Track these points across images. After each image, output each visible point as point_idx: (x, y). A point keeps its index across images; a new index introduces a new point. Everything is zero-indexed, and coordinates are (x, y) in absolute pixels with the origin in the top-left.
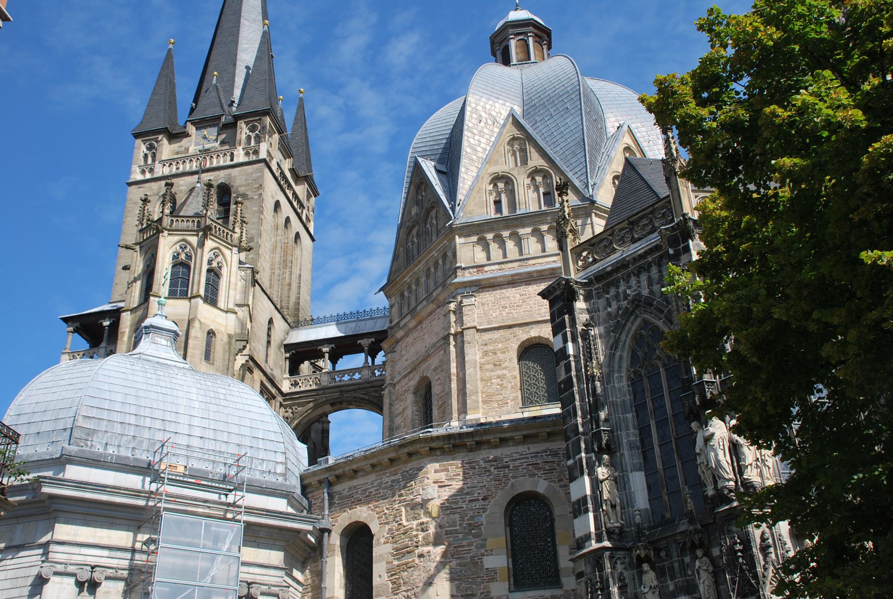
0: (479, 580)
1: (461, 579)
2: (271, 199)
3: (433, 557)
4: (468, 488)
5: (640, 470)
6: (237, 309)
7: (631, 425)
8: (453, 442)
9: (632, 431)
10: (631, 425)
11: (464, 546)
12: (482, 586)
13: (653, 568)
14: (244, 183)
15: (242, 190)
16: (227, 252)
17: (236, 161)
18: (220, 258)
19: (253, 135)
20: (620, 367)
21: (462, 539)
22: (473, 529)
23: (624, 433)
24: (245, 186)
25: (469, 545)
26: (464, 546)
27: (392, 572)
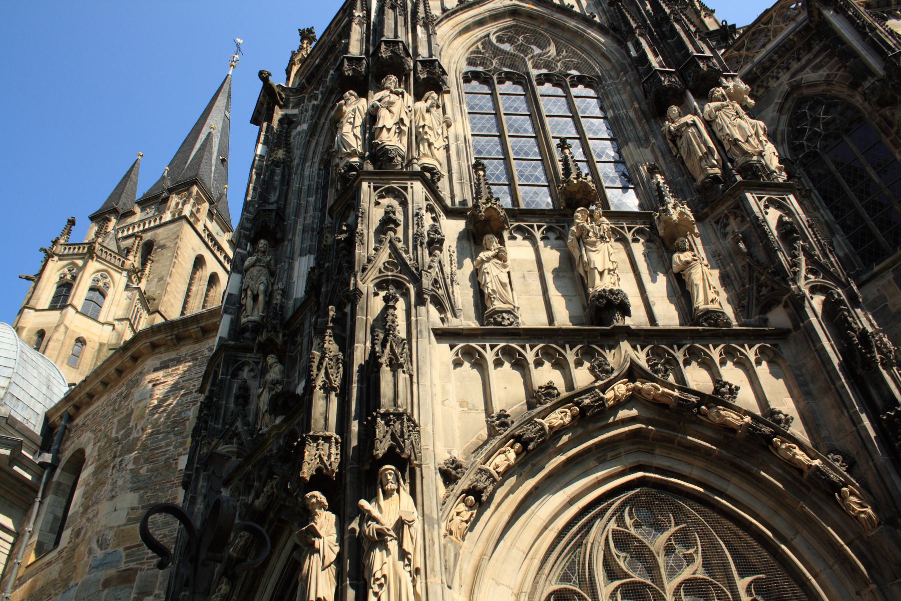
0: (168, 485)
1: (147, 487)
2: (191, 251)
3: (124, 465)
4: (183, 381)
5: (310, 253)
6: (116, 323)
7: (311, 208)
8: (175, 332)
9: (311, 212)
10: (311, 208)
11: (161, 447)
12: (170, 492)
13: (281, 361)
14: (165, 236)
15: (162, 242)
16: (116, 275)
17: (163, 221)
18: (107, 280)
19: (181, 202)
20: (314, 153)
21: (162, 440)
22: (176, 427)
23: (301, 221)
24: (165, 239)
25: (167, 445)
26: (161, 447)
27: (86, 495)
